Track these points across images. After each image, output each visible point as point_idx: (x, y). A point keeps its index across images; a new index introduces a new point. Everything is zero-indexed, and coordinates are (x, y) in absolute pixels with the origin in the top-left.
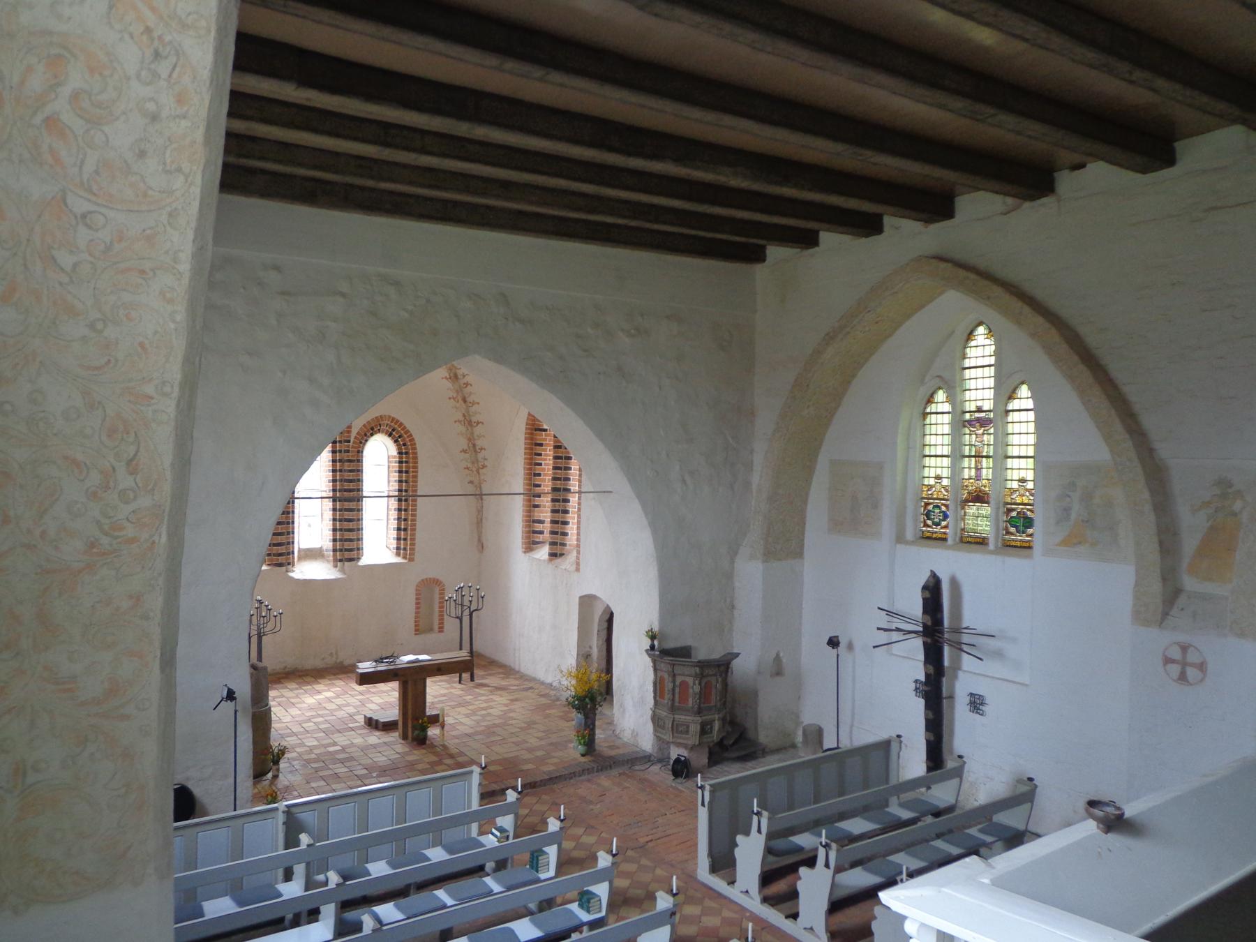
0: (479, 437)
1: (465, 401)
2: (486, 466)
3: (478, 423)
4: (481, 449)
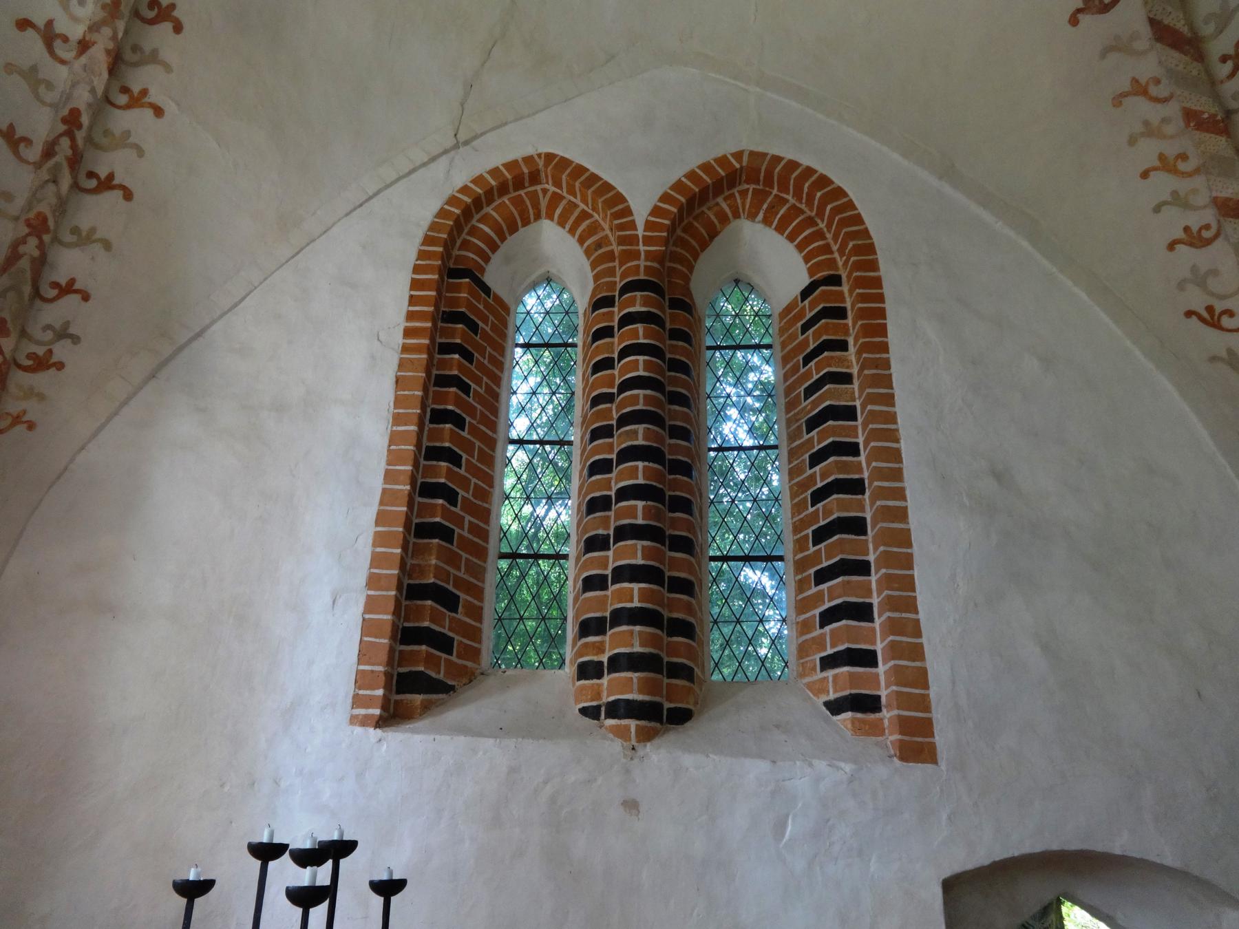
0: (84, 239)
1: (116, 62)
2: (60, 366)
3: (107, 184)
4: (68, 289)
